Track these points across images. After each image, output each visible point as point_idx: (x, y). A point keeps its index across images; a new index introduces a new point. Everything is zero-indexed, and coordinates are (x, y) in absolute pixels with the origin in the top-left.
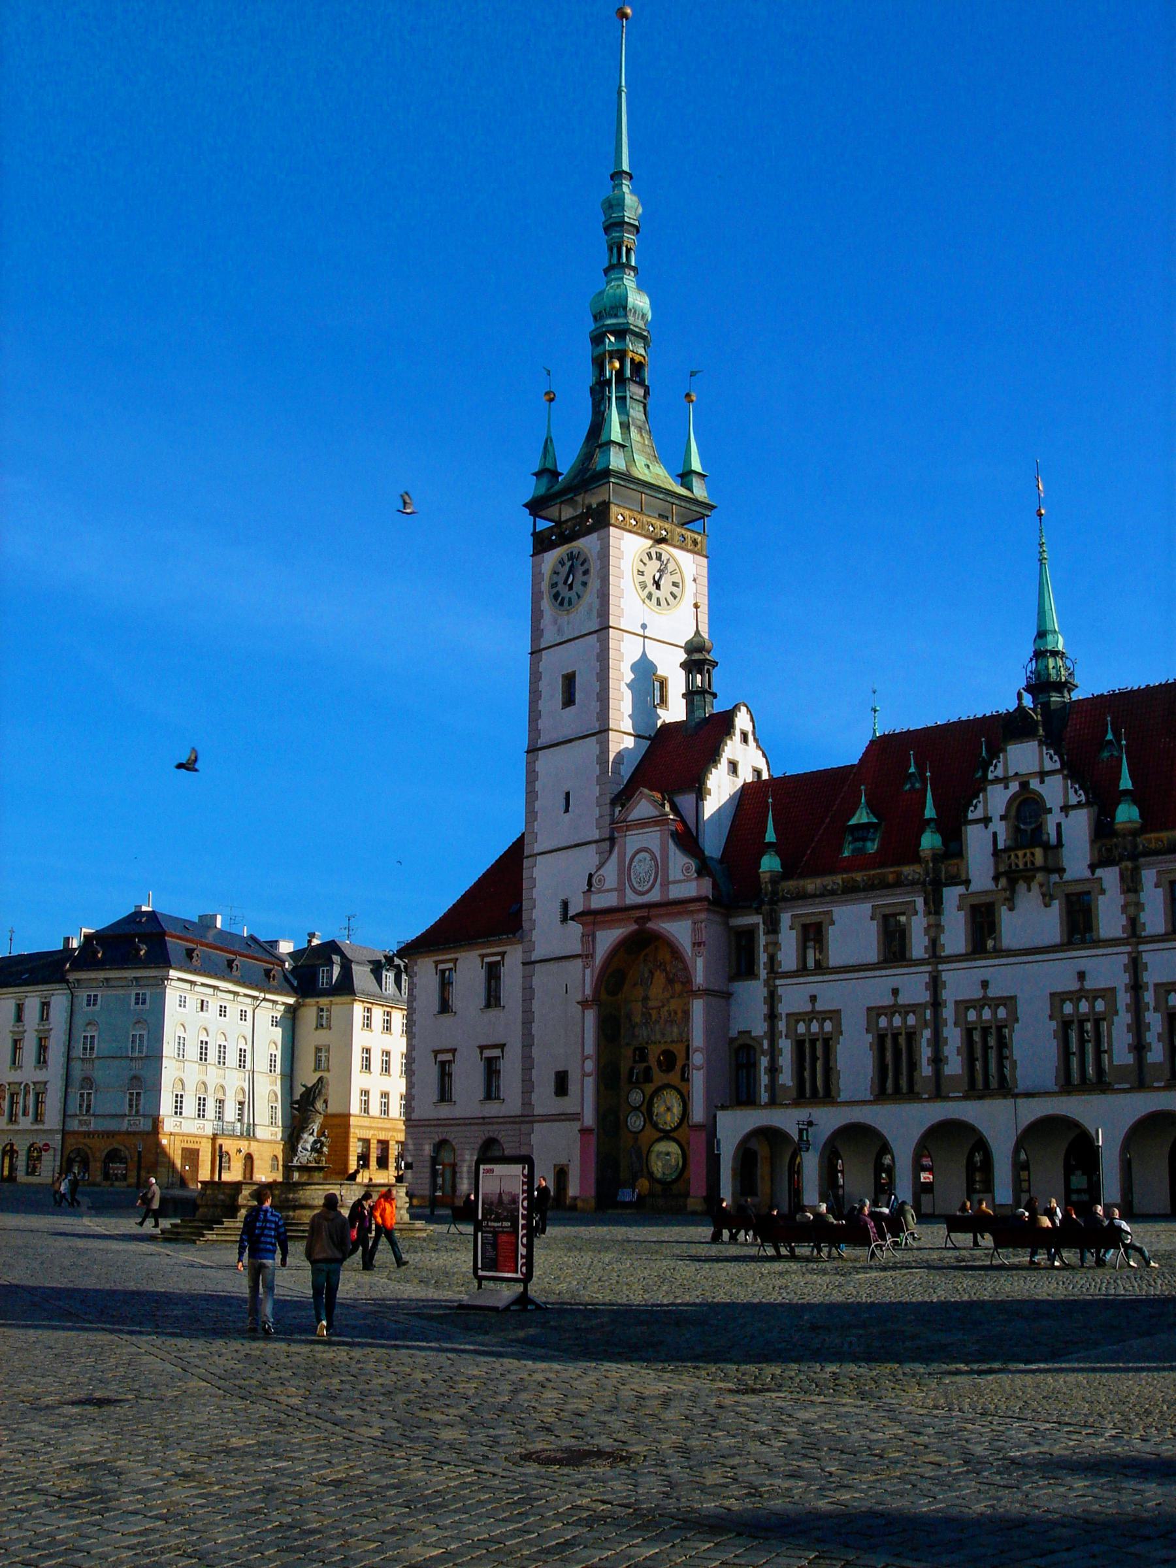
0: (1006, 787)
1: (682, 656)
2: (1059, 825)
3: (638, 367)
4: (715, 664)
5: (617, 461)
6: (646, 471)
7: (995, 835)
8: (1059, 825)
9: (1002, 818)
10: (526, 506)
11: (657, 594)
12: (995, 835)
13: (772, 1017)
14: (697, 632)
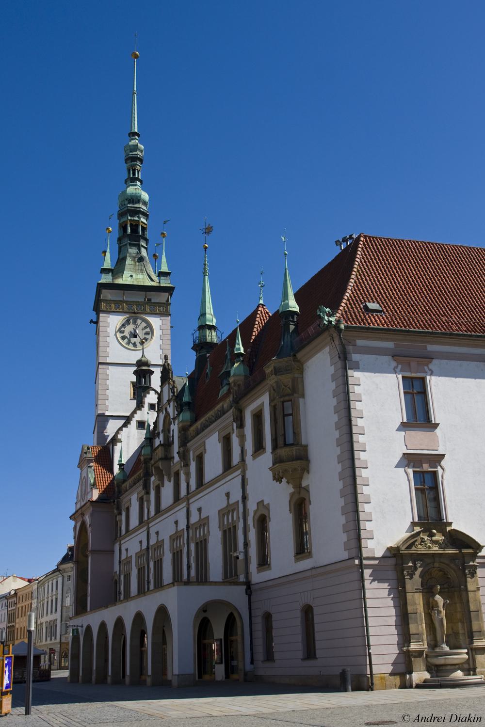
0: (163, 413)
1: (135, 368)
2: (173, 430)
3: (135, 226)
4: (152, 372)
5: (106, 279)
6: (129, 279)
7: (160, 442)
8: (173, 430)
9: (162, 431)
10: (93, 310)
11: (133, 340)
12: (160, 442)
13: (120, 562)
14: (143, 356)
